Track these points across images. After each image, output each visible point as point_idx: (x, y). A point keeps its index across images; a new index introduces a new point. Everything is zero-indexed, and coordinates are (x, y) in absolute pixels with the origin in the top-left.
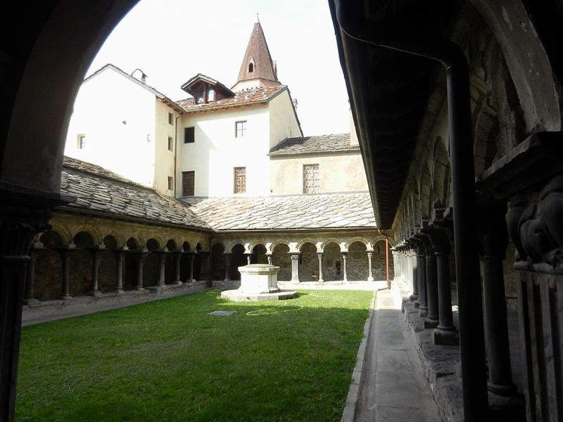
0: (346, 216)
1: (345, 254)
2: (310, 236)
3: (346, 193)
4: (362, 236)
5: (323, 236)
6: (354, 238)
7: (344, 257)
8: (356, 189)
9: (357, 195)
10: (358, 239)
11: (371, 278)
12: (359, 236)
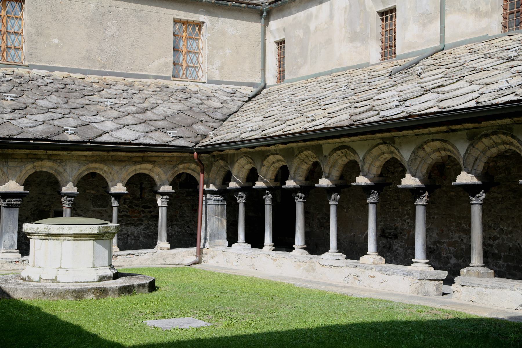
0: (123, 121)
1: (118, 196)
2: (49, 158)
3: (85, 72)
4: (153, 162)
5: (79, 160)
6: (138, 167)
7: (115, 203)
8: (104, 66)
9: (110, 79)
10: (145, 168)
11: (163, 244)
12: (149, 162)
